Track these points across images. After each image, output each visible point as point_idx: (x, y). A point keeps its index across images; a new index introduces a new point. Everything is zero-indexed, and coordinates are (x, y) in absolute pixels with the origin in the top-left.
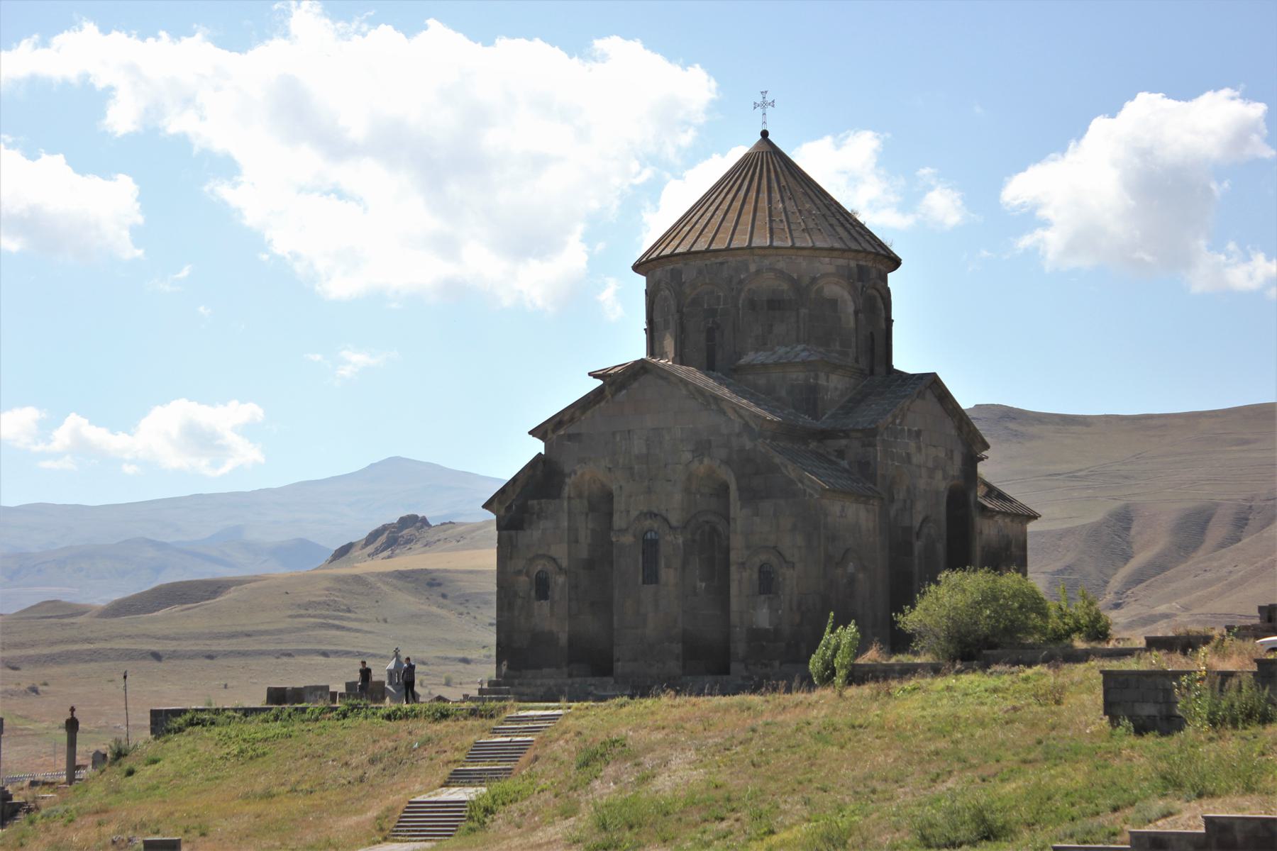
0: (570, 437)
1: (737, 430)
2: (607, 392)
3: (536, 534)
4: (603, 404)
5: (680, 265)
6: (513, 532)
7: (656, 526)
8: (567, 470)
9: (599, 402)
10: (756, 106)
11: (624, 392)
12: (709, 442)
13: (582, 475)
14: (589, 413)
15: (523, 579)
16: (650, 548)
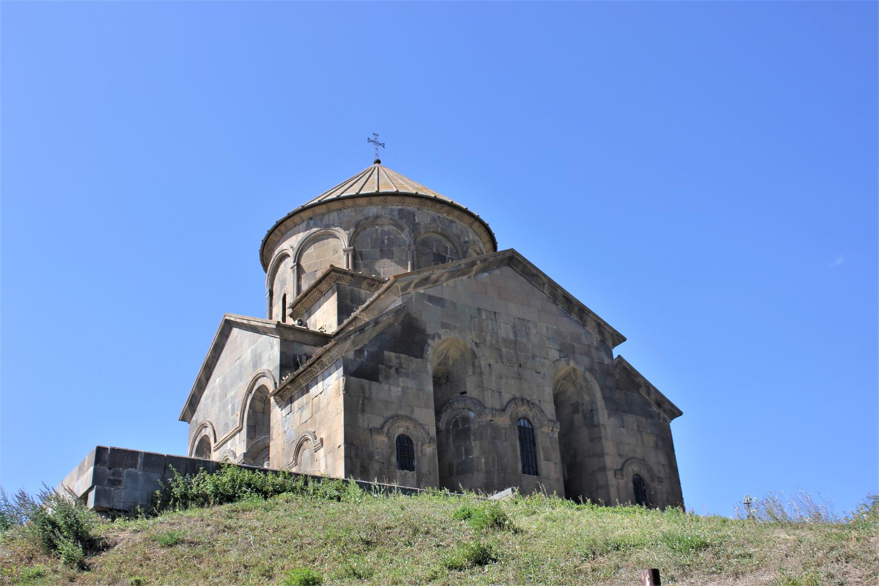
0: (431, 299)
1: (595, 344)
2: (475, 268)
3: (396, 391)
4: (465, 278)
5: (412, 208)
6: (365, 382)
7: (530, 415)
8: (430, 331)
9: (464, 274)
10: (369, 140)
11: (486, 274)
12: (574, 348)
13: (444, 341)
14: (451, 282)
15: (381, 440)
16: (527, 437)
